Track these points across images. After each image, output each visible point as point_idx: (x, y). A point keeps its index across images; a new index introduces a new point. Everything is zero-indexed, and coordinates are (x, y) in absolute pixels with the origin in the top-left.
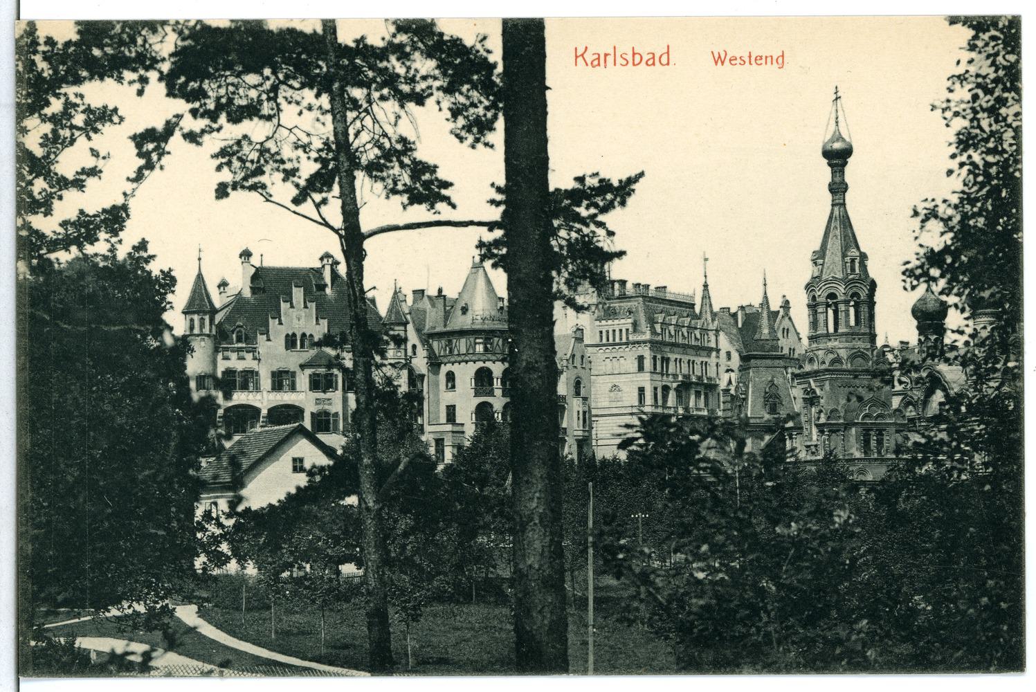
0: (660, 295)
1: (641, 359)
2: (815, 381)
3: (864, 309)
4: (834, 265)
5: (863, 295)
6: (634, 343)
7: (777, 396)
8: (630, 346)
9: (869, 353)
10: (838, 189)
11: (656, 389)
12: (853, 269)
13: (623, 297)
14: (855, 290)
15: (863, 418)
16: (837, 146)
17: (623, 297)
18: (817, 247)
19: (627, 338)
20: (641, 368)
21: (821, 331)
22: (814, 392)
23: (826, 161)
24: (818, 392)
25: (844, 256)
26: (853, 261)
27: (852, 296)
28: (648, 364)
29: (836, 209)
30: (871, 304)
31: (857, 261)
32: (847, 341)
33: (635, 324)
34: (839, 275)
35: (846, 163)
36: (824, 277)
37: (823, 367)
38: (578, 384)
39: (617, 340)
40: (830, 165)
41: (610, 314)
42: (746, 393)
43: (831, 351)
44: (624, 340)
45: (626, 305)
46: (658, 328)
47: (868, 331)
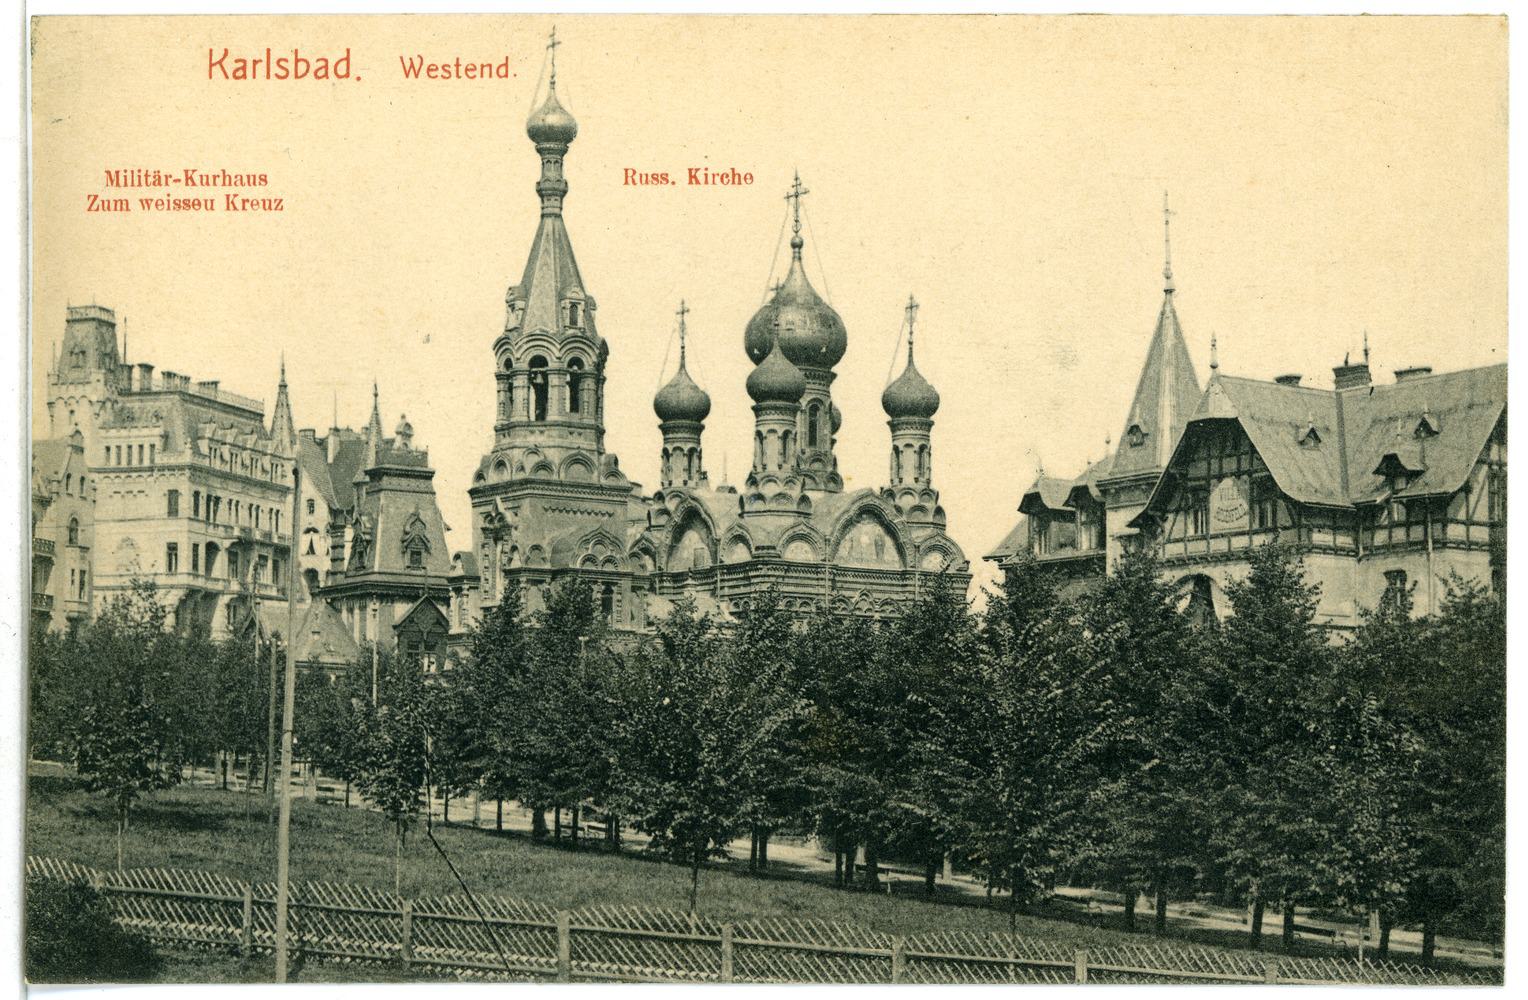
0: (208, 393)
1: (173, 495)
2: (504, 500)
3: (588, 384)
4: (543, 314)
5: (589, 361)
6: (162, 469)
7: (424, 542)
8: (156, 474)
9: (594, 458)
10: (552, 192)
11: (196, 546)
12: (574, 322)
13: (146, 392)
14: (576, 354)
15: (584, 562)
16: (553, 120)
17: (146, 392)
18: (516, 280)
19: (152, 461)
20: (173, 511)
21: (519, 416)
22: (502, 518)
23: (533, 145)
24: (509, 517)
25: (561, 297)
26: (574, 306)
27: (570, 364)
28: (185, 503)
29: (549, 222)
30: (600, 381)
31: (581, 308)
32: (561, 437)
33: (166, 437)
34: (552, 329)
35: (564, 151)
36: (527, 330)
37: (521, 476)
38: (73, 526)
39: (135, 463)
40: (539, 151)
41: (125, 419)
42: (372, 532)
43: (535, 451)
44: (146, 463)
45: (151, 405)
46: (204, 446)
47: (593, 422)
